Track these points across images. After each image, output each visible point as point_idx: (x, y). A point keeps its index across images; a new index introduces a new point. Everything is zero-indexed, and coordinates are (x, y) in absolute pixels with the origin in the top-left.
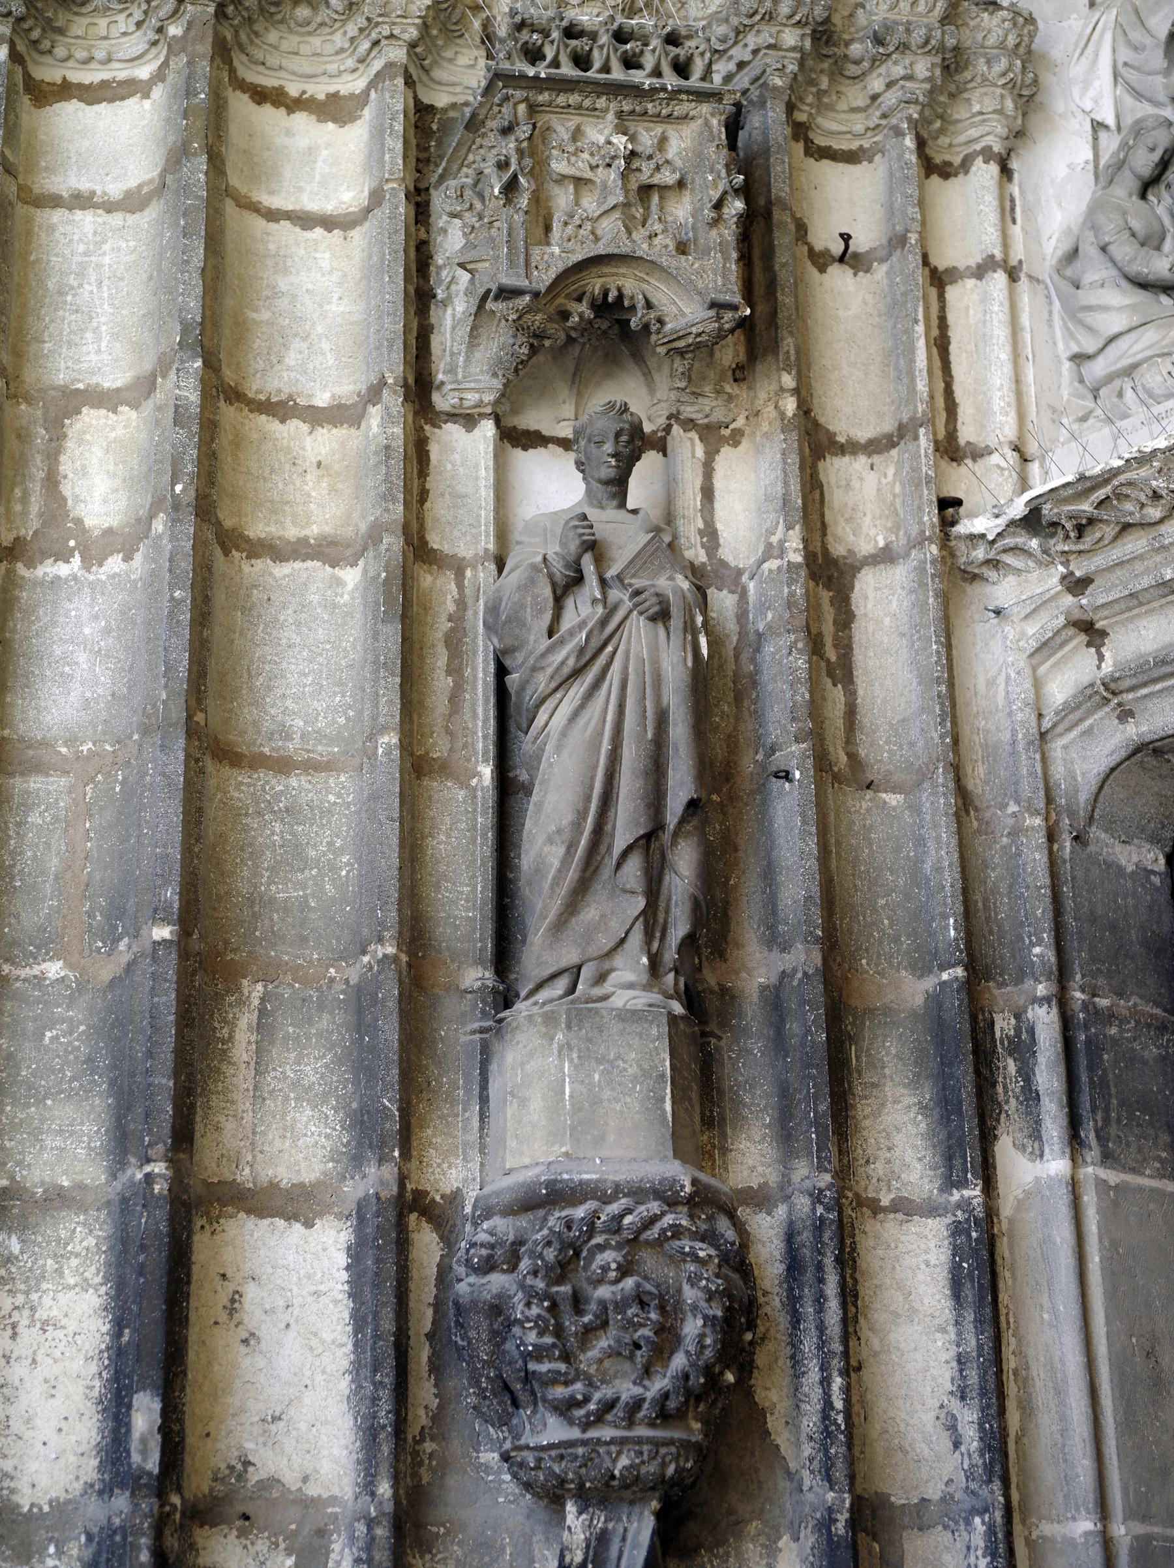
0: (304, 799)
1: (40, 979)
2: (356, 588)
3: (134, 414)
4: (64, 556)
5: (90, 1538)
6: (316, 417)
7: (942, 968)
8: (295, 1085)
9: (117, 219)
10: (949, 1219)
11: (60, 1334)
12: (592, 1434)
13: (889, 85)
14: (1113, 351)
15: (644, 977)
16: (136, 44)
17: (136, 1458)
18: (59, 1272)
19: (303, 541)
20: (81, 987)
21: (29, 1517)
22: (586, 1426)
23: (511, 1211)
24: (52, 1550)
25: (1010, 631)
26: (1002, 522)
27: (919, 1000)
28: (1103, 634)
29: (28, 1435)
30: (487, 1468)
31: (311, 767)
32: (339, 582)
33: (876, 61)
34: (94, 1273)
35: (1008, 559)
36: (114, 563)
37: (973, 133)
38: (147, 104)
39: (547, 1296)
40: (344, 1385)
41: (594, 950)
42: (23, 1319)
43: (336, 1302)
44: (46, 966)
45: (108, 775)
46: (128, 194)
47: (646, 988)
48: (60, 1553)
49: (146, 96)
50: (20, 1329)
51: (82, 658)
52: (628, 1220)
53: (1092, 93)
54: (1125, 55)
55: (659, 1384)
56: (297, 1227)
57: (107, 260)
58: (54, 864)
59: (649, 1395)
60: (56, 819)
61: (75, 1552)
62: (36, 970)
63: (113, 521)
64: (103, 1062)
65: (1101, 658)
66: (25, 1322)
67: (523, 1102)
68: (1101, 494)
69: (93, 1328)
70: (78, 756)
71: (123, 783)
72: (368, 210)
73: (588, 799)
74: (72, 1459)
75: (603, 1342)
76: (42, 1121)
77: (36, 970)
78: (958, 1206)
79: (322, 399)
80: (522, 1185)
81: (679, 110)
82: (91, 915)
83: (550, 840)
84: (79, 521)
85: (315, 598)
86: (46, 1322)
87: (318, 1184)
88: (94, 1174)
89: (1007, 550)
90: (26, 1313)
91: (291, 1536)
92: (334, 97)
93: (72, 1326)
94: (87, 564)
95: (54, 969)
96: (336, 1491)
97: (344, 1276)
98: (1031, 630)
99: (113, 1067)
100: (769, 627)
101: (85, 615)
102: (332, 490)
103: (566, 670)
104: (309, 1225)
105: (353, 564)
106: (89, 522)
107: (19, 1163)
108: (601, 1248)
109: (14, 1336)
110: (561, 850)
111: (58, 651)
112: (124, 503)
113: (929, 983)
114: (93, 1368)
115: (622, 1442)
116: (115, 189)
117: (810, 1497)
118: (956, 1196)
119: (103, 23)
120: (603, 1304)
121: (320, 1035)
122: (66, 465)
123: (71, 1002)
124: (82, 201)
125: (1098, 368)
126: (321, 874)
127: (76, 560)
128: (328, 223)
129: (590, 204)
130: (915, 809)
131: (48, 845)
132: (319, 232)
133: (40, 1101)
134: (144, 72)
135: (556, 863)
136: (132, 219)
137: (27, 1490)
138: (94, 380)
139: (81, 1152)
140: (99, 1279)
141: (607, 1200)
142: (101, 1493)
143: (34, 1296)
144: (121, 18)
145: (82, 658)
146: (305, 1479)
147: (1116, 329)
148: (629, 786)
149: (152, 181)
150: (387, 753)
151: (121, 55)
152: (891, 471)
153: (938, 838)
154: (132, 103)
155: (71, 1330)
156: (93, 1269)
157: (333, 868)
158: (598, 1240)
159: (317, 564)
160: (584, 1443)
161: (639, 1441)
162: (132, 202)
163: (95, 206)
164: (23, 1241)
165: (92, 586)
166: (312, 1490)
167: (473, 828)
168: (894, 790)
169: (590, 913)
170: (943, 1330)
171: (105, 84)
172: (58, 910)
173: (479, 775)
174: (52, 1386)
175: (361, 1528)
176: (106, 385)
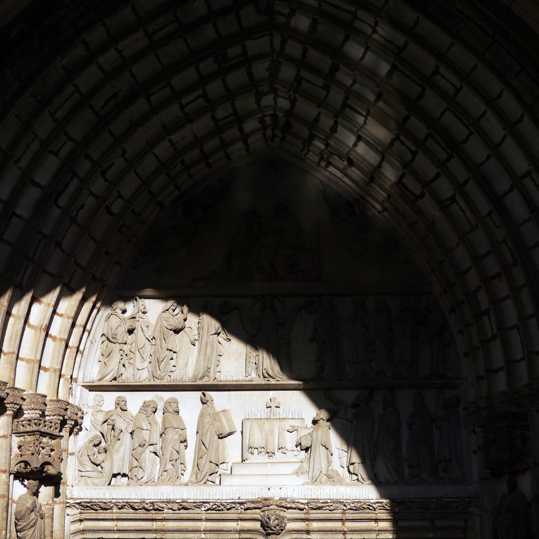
26: (74, 502)
35: (72, 507)
54: (93, 419)
65: (81, 524)
68: (92, 504)
98: (72, 517)
103: (32, 526)
125: (83, 474)
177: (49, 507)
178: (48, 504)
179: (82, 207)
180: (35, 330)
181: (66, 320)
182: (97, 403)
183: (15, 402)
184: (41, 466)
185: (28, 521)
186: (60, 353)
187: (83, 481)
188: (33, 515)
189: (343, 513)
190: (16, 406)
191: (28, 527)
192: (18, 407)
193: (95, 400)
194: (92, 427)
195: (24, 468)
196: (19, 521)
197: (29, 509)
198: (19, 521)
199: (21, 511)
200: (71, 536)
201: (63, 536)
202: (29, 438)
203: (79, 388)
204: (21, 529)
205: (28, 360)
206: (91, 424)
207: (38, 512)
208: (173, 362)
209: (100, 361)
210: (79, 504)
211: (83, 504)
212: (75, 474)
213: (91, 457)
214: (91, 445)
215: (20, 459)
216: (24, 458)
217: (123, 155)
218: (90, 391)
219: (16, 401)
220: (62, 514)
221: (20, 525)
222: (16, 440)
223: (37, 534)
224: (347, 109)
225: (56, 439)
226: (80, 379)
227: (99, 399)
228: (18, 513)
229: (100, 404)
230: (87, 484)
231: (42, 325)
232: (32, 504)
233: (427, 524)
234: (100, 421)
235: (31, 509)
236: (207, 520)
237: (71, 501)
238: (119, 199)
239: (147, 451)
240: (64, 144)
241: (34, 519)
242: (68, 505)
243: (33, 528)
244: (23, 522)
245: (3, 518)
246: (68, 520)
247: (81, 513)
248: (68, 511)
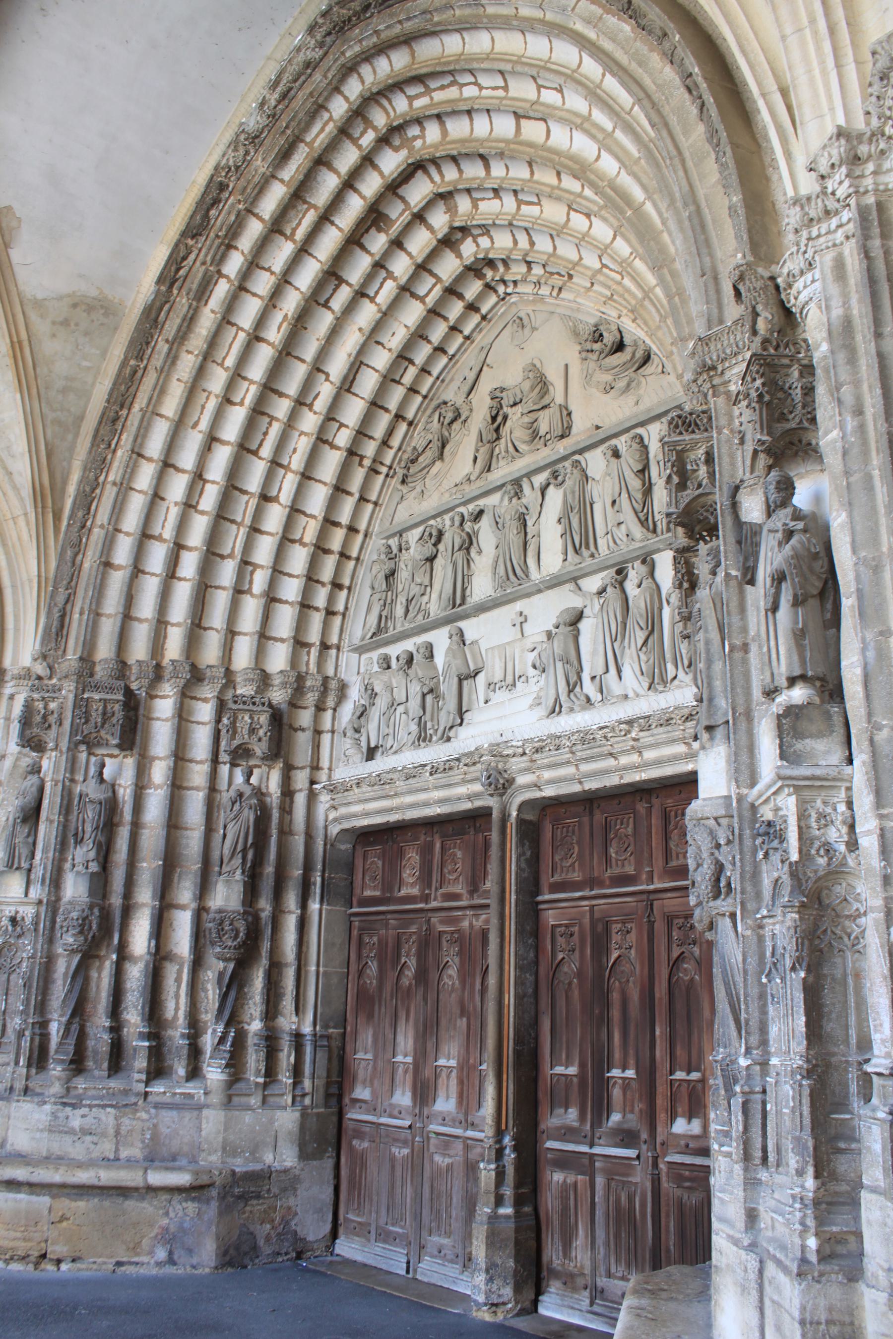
31: (191, 829)
34: (148, 918)
88: (149, 901)
124: (158, 719)
128: (203, 723)
148: (241, 840)
162: (166, 720)
169: (233, 862)
179: (295, 450)
189: (573, 753)
208: (425, 599)
217: (327, 379)
224: (523, 207)
233: (681, 749)
236: (437, 788)
238: (343, 429)
239: (398, 712)
240: (248, 390)
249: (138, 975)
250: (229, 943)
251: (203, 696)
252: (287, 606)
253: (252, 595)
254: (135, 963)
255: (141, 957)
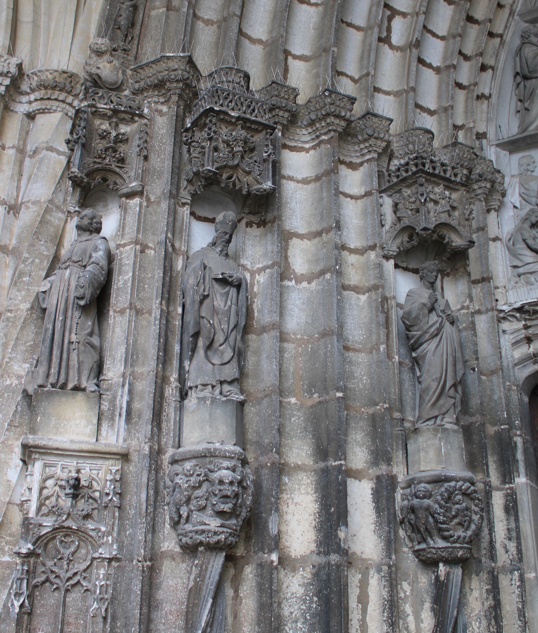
0: (354, 359)
1: (289, 403)
2: (365, 301)
3: (309, 242)
4: (290, 280)
5: (314, 566)
6: (352, 251)
7: (502, 425)
8: (355, 441)
9: (300, 185)
10: (504, 492)
11: (300, 507)
12: (454, 545)
13: (479, 188)
14: (527, 267)
15: (455, 421)
16: (308, 138)
17: (342, 545)
18: (299, 489)
19: (349, 285)
20: (301, 406)
21: (294, 559)
22: (454, 542)
23: (429, 482)
24: (301, 569)
25: (506, 336)
26: (511, 308)
27: (492, 433)
28: (532, 341)
29: (293, 536)
30: (405, 552)
31: (355, 350)
32: (359, 299)
33: (478, 181)
34: (311, 489)
35: (509, 318)
36: (305, 284)
37: (492, 203)
38: (308, 155)
39: (445, 507)
40: (372, 527)
41: (442, 412)
42: (290, 501)
43: (369, 504)
44: (291, 399)
45: (306, 345)
46: (303, 179)
47: (455, 424)
48: (304, 570)
49: (308, 152)
50: (289, 505)
51: (296, 310)
52: (463, 487)
53: (514, 198)
54: (523, 190)
55: (469, 533)
56: (357, 481)
57: (298, 196)
58: (292, 369)
59: (468, 535)
60: (292, 356)
61: (309, 570)
62: (288, 400)
63: (304, 272)
64: (310, 429)
65: (529, 347)
66: (290, 503)
67: (427, 452)
69: (311, 506)
70: (297, 339)
71: (311, 348)
72: (362, 197)
73: (442, 370)
74: (306, 543)
75: (456, 520)
76: (292, 444)
77: (288, 400)
78: (508, 488)
79: (352, 246)
80: (435, 475)
81: (457, 187)
82: (303, 385)
83: (433, 380)
84: (294, 270)
85: (353, 302)
86: (296, 503)
87: (362, 470)
88: (309, 462)
89: (510, 316)
90: (291, 500)
91: (360, 569)
92: (351, 162)
93: (304, 505)
94: (297, 283)
95: (293, 400)
96: (371, 557)
97: (371, 496)
98: (511, 337)
99: (314, 431)
100: (464, 328)
101: (297, 297)
102: (356, 272)
103: (434, 334)
104: (360, 481)
105: (364, 294)
106: (296, 271)
107: (287, 456)
108: (457, 494)
109: (288, 507)
110: (437, 384)
111: (290, 307)
112: (307, 267)
113: (496, 428)
114: (312, 518)
115: (461, 548)
116: (300, 177)
117: (485, 564)
118: (507, 486)
119: (298, 130)
120: (458, 510)
121: (360, 427)
122: (289, 253)
123: (299, 410)
124: (291, 178)
125: (521, 270)
126: (358, 381)
127: (294, 281)
128: (352, 197)
129: (439, 208)
130: (491, 381)
131: (290, 364)
132: (349, 199)
133: (291, 439)
134: (307, 146)
135: (435, 387)
136: (305, 186)
137: (293, 552)
138: (296, 230)
139: (304, 454)
140: (313, 492)
141: (457, 481)
142: (317, 554)
143: (293, 495)
144: (304, 130)
145: (296, 310)
146: (362, 553)
147: (529, 261)
149: (311, 177)
150: (384, 350)
151: (302, 140)
152: (479, 289)
153: (500, 390)
154: (303, 153)
155: (304, 506)
156: (310, 489)
157: (362, 380)
158: (457, 492)
159: (353, 292)
160: (452, 547)
161: (465, 548)
162: (305, 181)
163: (294, 181)
164: (289, 479)
165: (298, 289)
166: (364, 556)
167: (394, 373)
168: (484, 375)
169: (441, 402)
170: (502, 521)
171: (295, 147)
172: (293, 383)
173: (394, 358)
174: (299, 522)
175: (385, 568)
176: (300, 232)
177: (465, 311)
178: (463, 308)
180: (401, 51)
181: (451, 41)
182: (525, 166)
183: (376, 135)
184: (434, 228)
185: (425, 328)
186: (449, 84)
187: (522, 281)
188: (434, 318)
190: (379, 142)
191: (427, 336)
192: (384, 144)
193: (520, 165)
194: (524, 202)
195: (408, 242)
196: (411, 329)
197: (424, 305)
198: (411, 329)
199: (411, 312)
200: (517, 368)
201: (499, 363)
202: (407, 192)
203: (493, 149)
204: (415, 342)
205: (397, 92)
206: (520, 199)
207: (443, 311)
209: (519, 112)
210: (520, 310)
211: (526, 307)
212: (507, 274)
213: (530, 242)
214: (527, 226)
215: (398, 227)
216: (406, 222)
218: (511, 152)
219: (379, 133)
220: (493, 328)
221: (413, 336)
222: (388, 202)
223: (445, 348)
225: (458, 190)
226: (491, 135)
227: (525, 161)
228: (406, 316)
229: (530, 168)
230: (528, 283)
231: (411, 42)
232: (429, 298)
234: (534, 190)
235: (429, 305)
237: (506, 308)
241: (437, 322)
242: (502, 315)
243: (437, 339)
244: (417, 331)
245: (378, 323)
246: (506, 341)
247: (526, 327)
248: (505, 326)
249: (301, 591)
250: (460, 533)
251: (348, 160)
252: (431, 71)
253: (391, 46)
254: (294, 570)
255: (304, 559)
